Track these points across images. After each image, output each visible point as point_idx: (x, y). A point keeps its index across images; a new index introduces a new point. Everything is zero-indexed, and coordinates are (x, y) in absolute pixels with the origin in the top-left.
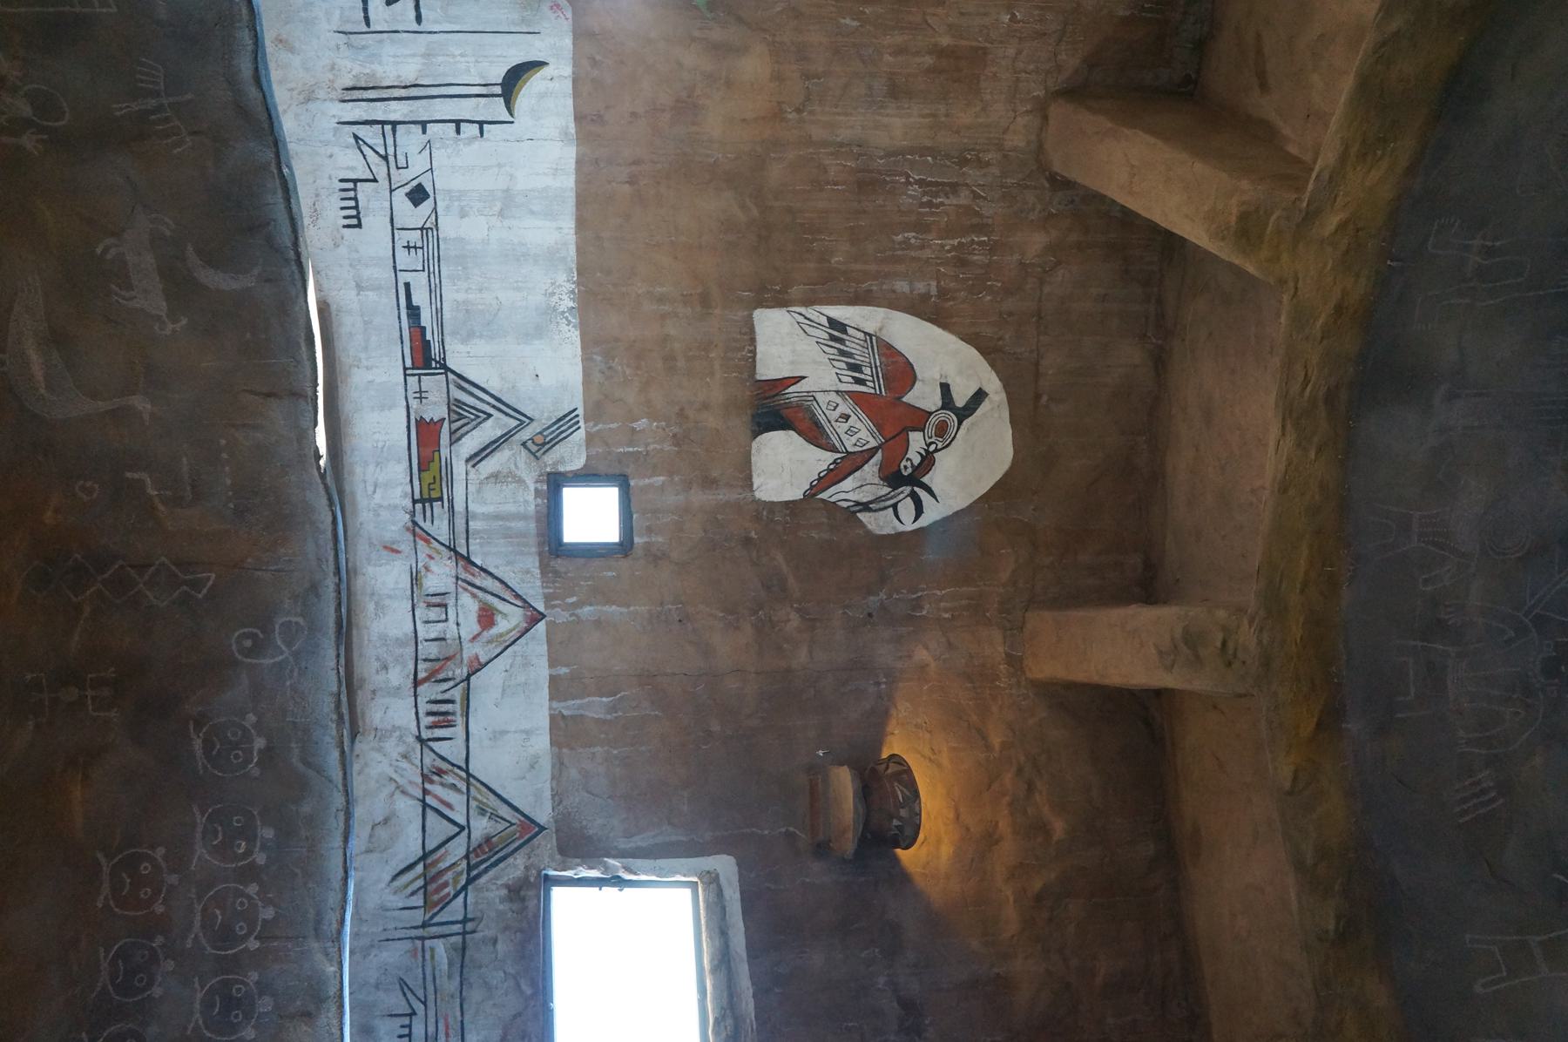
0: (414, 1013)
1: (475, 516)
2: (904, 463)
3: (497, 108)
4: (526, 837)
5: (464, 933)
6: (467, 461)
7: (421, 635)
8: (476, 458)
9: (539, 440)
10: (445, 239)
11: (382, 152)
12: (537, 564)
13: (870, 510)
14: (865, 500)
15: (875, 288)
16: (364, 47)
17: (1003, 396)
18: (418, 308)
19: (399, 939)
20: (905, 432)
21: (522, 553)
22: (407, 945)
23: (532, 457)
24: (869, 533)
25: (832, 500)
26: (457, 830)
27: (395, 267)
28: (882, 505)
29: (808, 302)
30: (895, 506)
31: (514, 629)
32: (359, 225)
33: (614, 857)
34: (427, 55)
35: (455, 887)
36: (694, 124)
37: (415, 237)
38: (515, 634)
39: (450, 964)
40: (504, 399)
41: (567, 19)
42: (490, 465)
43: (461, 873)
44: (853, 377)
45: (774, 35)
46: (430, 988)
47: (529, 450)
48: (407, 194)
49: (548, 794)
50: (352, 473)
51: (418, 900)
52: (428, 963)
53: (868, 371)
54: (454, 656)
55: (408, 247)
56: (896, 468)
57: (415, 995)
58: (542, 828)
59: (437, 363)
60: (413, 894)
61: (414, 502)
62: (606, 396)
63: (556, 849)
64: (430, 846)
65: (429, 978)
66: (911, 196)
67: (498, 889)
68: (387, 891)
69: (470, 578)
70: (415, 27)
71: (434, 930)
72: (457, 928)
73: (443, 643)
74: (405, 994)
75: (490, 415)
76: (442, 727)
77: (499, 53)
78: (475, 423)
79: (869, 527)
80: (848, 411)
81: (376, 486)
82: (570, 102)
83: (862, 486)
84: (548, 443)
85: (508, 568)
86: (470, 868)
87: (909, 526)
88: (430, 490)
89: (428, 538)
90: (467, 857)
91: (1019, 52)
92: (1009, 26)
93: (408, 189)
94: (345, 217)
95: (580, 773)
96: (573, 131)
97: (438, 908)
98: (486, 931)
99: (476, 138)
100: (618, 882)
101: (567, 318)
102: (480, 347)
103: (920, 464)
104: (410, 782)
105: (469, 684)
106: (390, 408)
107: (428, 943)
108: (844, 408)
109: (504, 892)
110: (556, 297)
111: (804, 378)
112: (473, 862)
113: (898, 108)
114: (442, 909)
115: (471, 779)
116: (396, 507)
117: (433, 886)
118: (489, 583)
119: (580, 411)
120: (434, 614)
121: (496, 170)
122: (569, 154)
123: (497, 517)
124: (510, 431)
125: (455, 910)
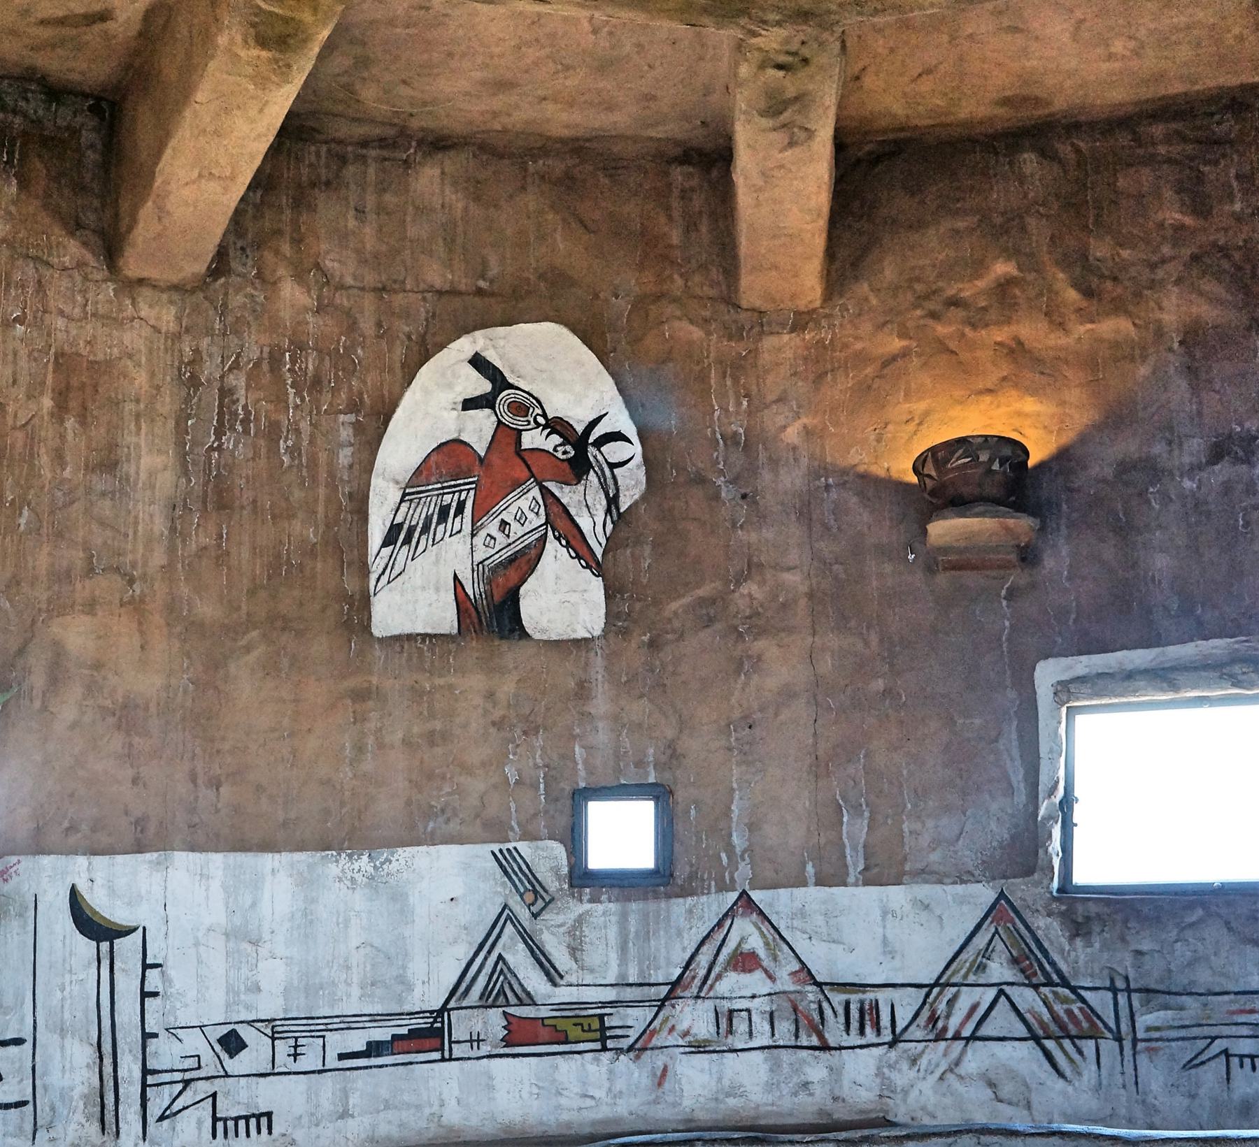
0: (1226, 1053)
1: (623, 975)
2: (559, 455)
3: (127, 947)
4: (1012, 914)
5: (1129, 990)
6: (555, 984)
7: (766, 1041)
8: (552, 974)
9: (529, 897)
10: (285, 1011)
11: (180, 1087)
12: (681, 900)
13: (617, 496)
14: (604, 502)
15: (347, 490)
16: (53, 1109)
17: (478, 334)
18: (369, 1044)
19: (1136, 1069)
20: (524, 454)
21: (668, 918)
22: (1143, 1060)
23: (551, 906)
24: (644, 498)
25: (604, 542)
26: (1003, 999)
27: (320, 1072)
28: (610, 482)
29: (365, 570)
30: (612, 466)
31: (759, 929)
32: (269, 1115)
33: (1037, 808)
34: (62, 1032)
35: (1073, 1002)
36: (147, 709)
37: (283, 1047)
38: (765, 928)
39: (1166, 1007)
40: (480, 940)
41: (19, 862)
42: (561, 958)
43: (1055, 993)
44: (455, 516)
45: (40, 610)
46: (1196, 1031)
47: (543, 909)
48: (231, 1057)
49: (959, 888)
50: (569, 1125)
51: (1088, 1046)
52: (1165, 1034)
53: (448, 498)
54: (792, 1001)
55: (295, 1056)
56: (566, 464)
57: (1204, 1050)
58: (1002, 895)
59: (435, 1021)
60: (1080, 1052)
61: (604, 1049)
62: (477, 816)
63: (1027, 879)
64: (1021, 1031)
65: (1183, 1033)
66: (236, 446)
67: (1075, 950)
68: (1077, 1084)
69: (697, 982)
70: (28, 1046)
71: (1125, 1027)
72: (1122, 999)
73: (776, 1014)
74: (1203, 1063)
75: (500, 957)
76: (878, 1017)
77: (60, 944)
78: (509, 976)
79: (636, 497)
80: (497, 522)
81: (586, 1096)
82: (120, 859)
83: (587, 506)
84: (533, 886)
85: (685, 935)
86: (1050, 983)
87: (636, 449)
88: (590, 1030)
89: (648, 1032)
90: (1036, 987)
91: (61, 313)
92: (29, 325)
93: (224, 1056)
94: (259, 1132)
95: (934, 850)
96: (155, 855)
97: (1098, 1022)
98: (1125, 962)
99: (163, 973)
100: (1067, 804)
101: (382, 864)
102: (417, 969)
103: (561, 436)
104: (945, 1055)
105: (826, 984)
106: (491, 1078)
107: (1140, 1035)
108: (493, 528)
109: (1079, 942)
110: (356, 876)
111: (456, 577)
112: (1042, 980)
113: (128, 461)
114: (1099, 1017)
115: (942, 981)
116: (611, 1072)
117: (1073, 1030)
118: (704, 959)
119: (496, 847)
120: (741, 1026)
121: (202, 949)
122: (182, 859)
123: (623, 949)
124: (519, 932)
125: (1100, 1001)
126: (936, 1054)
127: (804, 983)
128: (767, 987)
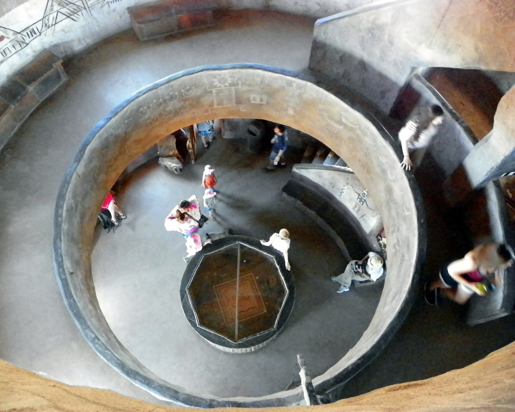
7: (15, 51)
22: (92, 12)
26: (59, 13)
43: (69, 6)
51: (80, 13)
52: (94, 4)
57: (103, 3)
60: (78, 15)
64: (65, 17)
76: (34, 31)
86: (67, 5)
90: (65, 7)
105: (21, 32)
114: (80, 6)
115: (45, 16)
117: (76, 12)
120: (7, 52)
126: (50, 31)
127: (16, 34)
128: (9, 40)
